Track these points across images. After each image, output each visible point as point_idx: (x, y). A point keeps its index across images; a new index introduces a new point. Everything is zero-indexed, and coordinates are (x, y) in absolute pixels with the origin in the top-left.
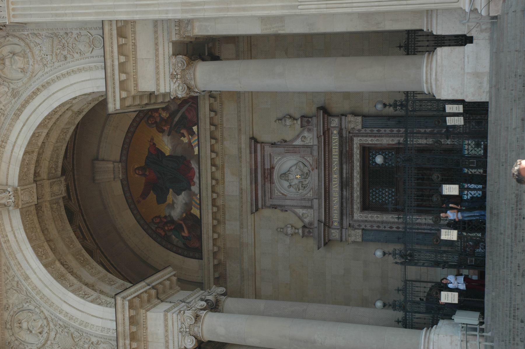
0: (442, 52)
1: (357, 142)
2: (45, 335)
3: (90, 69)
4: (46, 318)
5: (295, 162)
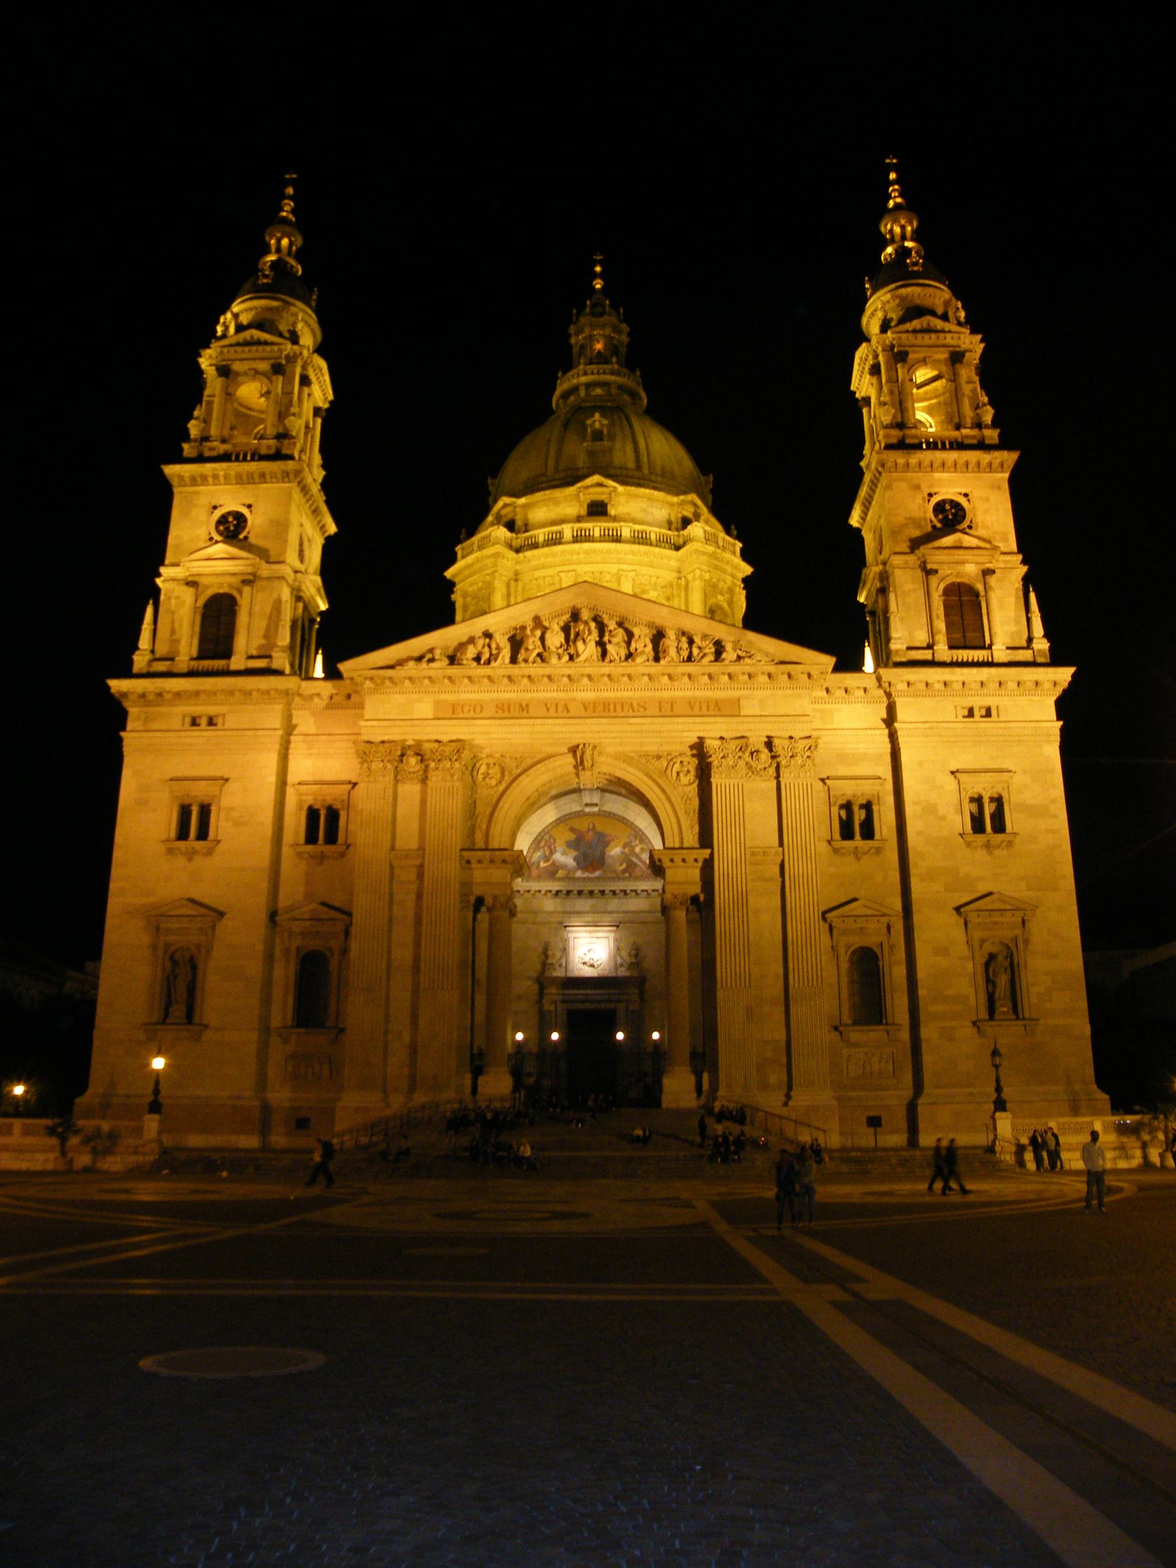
0: (692, 1079)
1: (622, 1005)
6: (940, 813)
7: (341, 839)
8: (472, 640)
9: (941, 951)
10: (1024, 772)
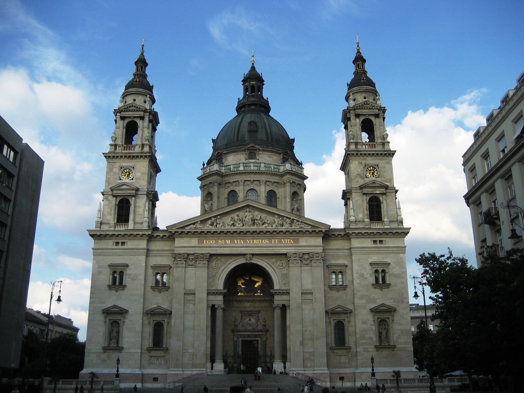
0: (282, 364)
1: (260, 339)
2: (215, 268)
3: (279, 284)
4: (219, 268)
5: (253, 322)
6: (365, 276)
7: (167, 285)
8: (210, 218)
9: (364, 323)
10: (394, 263)
